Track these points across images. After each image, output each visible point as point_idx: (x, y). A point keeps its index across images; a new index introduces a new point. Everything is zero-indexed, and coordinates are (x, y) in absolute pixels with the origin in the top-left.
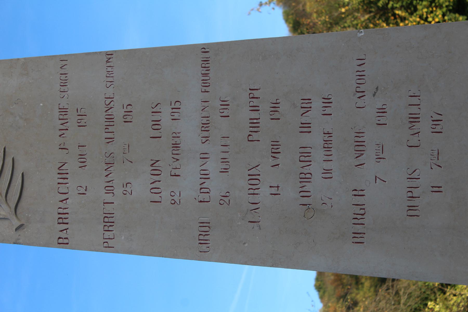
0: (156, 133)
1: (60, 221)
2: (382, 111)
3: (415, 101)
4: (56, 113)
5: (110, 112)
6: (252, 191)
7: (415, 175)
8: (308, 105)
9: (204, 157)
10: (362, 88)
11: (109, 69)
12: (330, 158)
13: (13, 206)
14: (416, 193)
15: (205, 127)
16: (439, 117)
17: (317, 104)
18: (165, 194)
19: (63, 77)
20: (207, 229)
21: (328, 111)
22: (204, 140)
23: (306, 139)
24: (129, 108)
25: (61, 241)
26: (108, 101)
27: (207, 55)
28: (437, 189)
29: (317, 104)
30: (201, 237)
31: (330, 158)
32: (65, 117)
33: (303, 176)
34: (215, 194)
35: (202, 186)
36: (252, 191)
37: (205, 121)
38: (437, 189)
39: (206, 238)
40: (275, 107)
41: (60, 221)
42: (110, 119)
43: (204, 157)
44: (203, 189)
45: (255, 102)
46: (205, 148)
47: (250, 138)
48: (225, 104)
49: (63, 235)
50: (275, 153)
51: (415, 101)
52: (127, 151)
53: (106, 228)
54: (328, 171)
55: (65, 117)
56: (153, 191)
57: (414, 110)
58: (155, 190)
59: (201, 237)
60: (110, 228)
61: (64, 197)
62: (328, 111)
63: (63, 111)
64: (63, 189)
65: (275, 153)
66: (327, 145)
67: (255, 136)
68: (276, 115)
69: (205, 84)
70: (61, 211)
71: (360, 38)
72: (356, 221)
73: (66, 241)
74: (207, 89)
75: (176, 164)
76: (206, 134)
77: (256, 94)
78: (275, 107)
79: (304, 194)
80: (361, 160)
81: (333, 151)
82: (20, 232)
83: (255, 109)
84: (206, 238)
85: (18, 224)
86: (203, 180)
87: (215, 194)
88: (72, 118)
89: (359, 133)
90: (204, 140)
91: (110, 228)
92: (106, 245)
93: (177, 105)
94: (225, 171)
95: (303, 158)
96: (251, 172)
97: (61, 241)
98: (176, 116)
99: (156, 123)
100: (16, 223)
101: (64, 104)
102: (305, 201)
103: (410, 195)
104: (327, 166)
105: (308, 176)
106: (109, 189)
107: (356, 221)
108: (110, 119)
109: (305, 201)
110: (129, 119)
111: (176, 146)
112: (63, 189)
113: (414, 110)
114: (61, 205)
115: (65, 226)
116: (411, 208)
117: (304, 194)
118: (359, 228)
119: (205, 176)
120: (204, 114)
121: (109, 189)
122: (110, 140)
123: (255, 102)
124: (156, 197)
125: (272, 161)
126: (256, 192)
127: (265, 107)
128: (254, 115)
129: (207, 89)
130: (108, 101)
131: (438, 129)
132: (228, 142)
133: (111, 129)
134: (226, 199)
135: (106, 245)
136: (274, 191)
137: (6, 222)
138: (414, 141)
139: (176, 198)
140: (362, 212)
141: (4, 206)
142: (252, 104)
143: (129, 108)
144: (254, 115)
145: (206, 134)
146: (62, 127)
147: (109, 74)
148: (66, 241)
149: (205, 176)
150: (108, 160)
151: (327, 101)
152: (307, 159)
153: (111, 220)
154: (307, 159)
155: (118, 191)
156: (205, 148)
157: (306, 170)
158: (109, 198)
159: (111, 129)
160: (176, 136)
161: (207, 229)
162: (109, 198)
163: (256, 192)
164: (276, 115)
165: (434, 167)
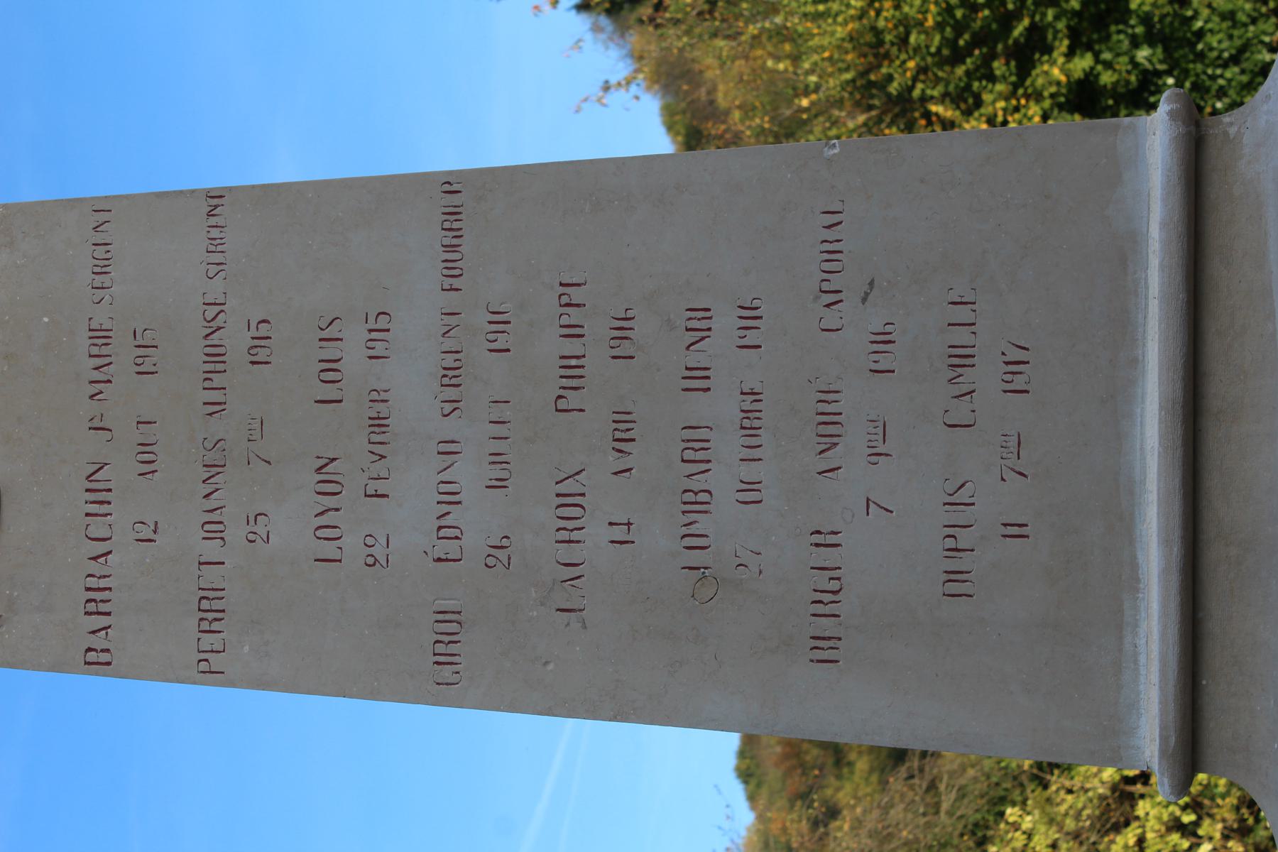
0: (330, 392)
1: (92, 607)
2: (883, 339)
3: (963, 314)
5: (214, 339)
6: (564, 535)
7: (962, 496)
8: (704, 325)
9: (448, 449)
10: (836, 282)
11: (215, 233)
12: (756, 453)
14: (964, 541)
15: (451, 376)
16: (1021, 355)
17: (725, 322)
18: (352, 543)
19: (100, 252)
20: (453, 627)
21: (752, 337)
22: (448, 408)
23: (699, 408)
25: (92, 656)
27: (455, 199)
28: (1016, 531)
29: (725, 322)
30: (440, 648)
31: (756, 453)
32: (105, 351)
33: (689, 497)
34: (475, 541)
35: (443, 522)
36: (564, 535)
37: (449, 361)
38: (1016, 531)
39: (453, 648)
41: (92, 607)
42: (215, 356)
43: (448, 449)
45: (574, 316)
46: (450, 428)
47: (562, 404)
48: (499, 321)
49: (98, 641)
50: (622, 442)
51: (963, 314)
52: (257, 435)
53: (205, 626)
54: (750, 486)
55: (105, 351)
56: (320, 533)
57: (962, 336)
58: (326, 531)
59: (440, 648)
60: (215, 626)
61: (101, 547)
62: (752, 337)
63: (100, 336)
65: (622, 442)
66: (749, 426)
67: (573, 399)
68: (626, 349)
69: (452, 270)
70: (92, 582)
71: (830, 160)
72: (820, 609)
73: (104, 657)
74: (456, 283)
75: (379, 468)
76: (452, 393)
77: (576, 295)
78: (622, 328)
80: (833, 458)
81: (765, 437)
83: (573, 332)
84: (453, 648)
86: (445, 508)
87: (475, 541)
88: (123, 354)
90: (448, 408)
91: (215, 626)
92: (203, 666)
94: (499, 484)
95: (689, 455)
96: (562, 488)
97: (92, 656)
98: (380, 348)
99: (330, 366)
101: (101, 319)
102: (696, 558)
103: (950, 543)
105: (703, 497)
106: (213, 529)
107: (820, 609)
108: (215, 356)
109: (696, 558)
111: (378, 423)
113: (962, 336)
114: (94, 567)
115: (102, 621)
116: (953, 575)
117: (693, 541)
119: (450, 499)
120: (449, 344)
121: (213, 529)
122: (214, 409)
123: (574, 316)
124: (329, 550)
126: (575, 535)
127: (598, 328)
129: (456, 283)
131: (1019, 383)
132: (506, 412)
133: (218, 380)
134: (501, 554)
135: (203, 666)
136: (619, 534)
138: (961, 412)
139: (378, 551)
140: (834, 585)
142: (565, 320)
146: (97, 375)
147: (215, 246)
148: (104, 657)
149: (450, 499)
151: (750, 314)
152: (700, 455)
153: (217, 605)
154: (700, 455)
155: (236, 533)
156: (450, 428)
158: (212, 550)
159: (218, 380)
160: (379, 397)
161: (453, 627)
162: (212, 550)
163: (575, 535)
164: (626, 349)
165: (1010, 475)
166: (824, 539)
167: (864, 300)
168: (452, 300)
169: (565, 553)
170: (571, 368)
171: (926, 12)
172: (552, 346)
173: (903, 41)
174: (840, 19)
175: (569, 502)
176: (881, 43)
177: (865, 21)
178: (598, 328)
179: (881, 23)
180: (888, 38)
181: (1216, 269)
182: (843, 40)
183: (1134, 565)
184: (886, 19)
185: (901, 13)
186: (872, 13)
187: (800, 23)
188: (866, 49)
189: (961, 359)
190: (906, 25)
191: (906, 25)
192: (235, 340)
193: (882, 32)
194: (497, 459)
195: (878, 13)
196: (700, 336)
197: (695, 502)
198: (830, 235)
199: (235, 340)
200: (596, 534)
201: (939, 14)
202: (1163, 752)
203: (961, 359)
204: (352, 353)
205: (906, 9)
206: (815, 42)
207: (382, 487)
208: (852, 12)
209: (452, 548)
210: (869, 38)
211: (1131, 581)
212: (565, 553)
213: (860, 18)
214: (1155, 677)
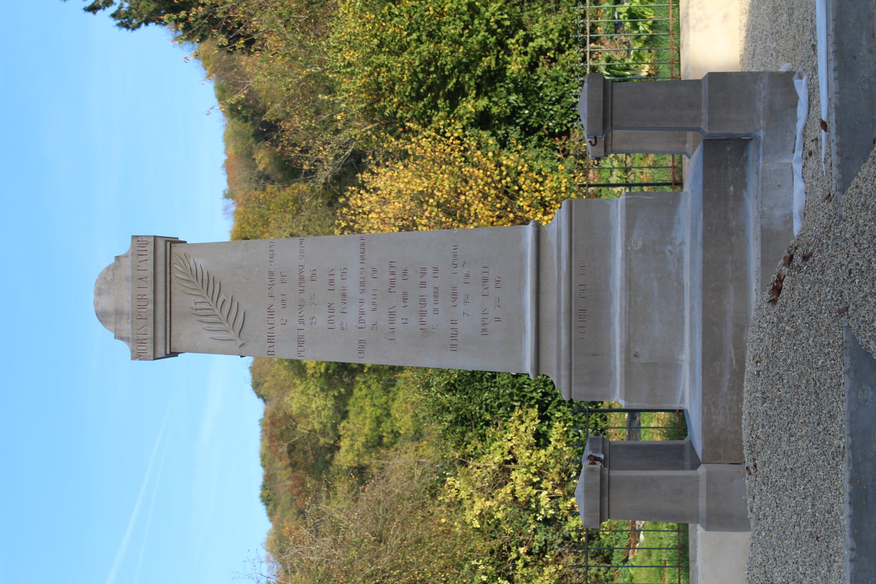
0: (331, 287)
2: (467, 276)
3: (486, 270)
4: (267, 275)
5: (302, 274)
7: (485, 312)
9: (362, 301)
13: (238, 332)
14: (486, 321)
15: (362, 284)
16: (499, 279)
17: (430, 271)
18: (337, 324)
19: (271, 253)
20: (363, 344)
21: (436, 275)
23: (424, 291)
24: (314, 272)
25: (269, 353)
26: (301, 268)
27: (363, 241)
28: (498, 319)
29: (430, 271)
38: (498, 319)
40: (405, 272)
42: (302, 278)
43: (362, 301)
44: (360, 321)
45: (393, 270)
46: (362, 296)
50: (405, 299)
51: (486, 270)
54: (436, 310)
57: (485, 275)
58: (331, 321)
61: (272, 326)
62: (436, 275)
63: (271, 273)
64: (271, 321)
65: (405, 299)
66: (436, 296)
67: (393, 289)
68: (406, 277)
69: (363, 258)
70: (269, 335)
75: (344, 306)
76: (363, 288)
77: (394, 264)
78: (405, 272)
79: (423, 323)
81: (439, 298)
82: (242, 348)
83: (393, 273)
85: (242, 343)
88: (277, 278)
89: (454, 288)
93: (345, 271)
94: (375, 310)
96: (390, 310)
97: (269, 353)
99: (332, 281)
100: (240, 342)
101: (272, 269)
102: (423, 327)
104: (436, 306)
106: (302, 321)
108: (302, 278)
109: (423, 327)
110: (314, 278)
111: (344, 295)
112: (271, 321)
113: (485, 275)
115: (272, 344)
116: (484, 330)
117: (423, 323)
118: (454, 342)
119: (362, 313)
121: (302, 321)
122: (302, 291)
123: (393, 270)
124: (331, 326)
125: (403, 304)
127: (399, 273)
128: (392, 277)
130: (301, 268)
132: (377, 293)
133: (302, 285)
134: (375, 326)
136: (404, 321)
137: (233, 342)
138: (485, 292)
139: (344, 326)
141: (231, 332)
143: (314, 272)
144: (392, 277)
145: (363, 288)
146: (270, 283)
147: (302, 252)
149: (362, 313)
150: (300, 304)
151: (436, 270)
155: (307, 322)
156: (362, 296)
157: (423, 309)
158: (301, 326)
159: (302, 285)
161: (363, 344)
162: (301, 326)
164: (406, 277)
166: (453, 322)
167: (463, 266)
168: (363, 266)
169: (391, 326)
170: (392, 282)
171: (404, 74)
172: (387, 277)
173: (392, 90)
174: (359, 77)
175: (392, 314)
176: (381, 89)
177: (372, 78)
178: (399, 273)
179: (380, 80)
180: (384, 87)
181: (542, 260)
182: (361, 87)
183: (525, 327)
184: (383, 77)
185: (391, 75)
186: (376, 74)
187: (335, 78)
188: (372, 92)
189: (485, 280)
190: (393, 81)
191: (393, 81)
192: (307, 275)
193: (381, 83)
194: (374, 303)
195: (379, 74)
196: (424, 274)
197: (423, 314)
198: (455, 251)
199: (307, 275)
200: (398, 321)
201: (410, 75)
202: (531, 369)
203: (485, 280)
204: (337, 278)
205: (394, 73)
206: (344, 87)
207: (345, 311)
208: (366, 73)
209: (363, 325)
210: (374, 86)
211: (523, 330)
212: (391, 326)
213: (369, 76)
214: (529, 352)
